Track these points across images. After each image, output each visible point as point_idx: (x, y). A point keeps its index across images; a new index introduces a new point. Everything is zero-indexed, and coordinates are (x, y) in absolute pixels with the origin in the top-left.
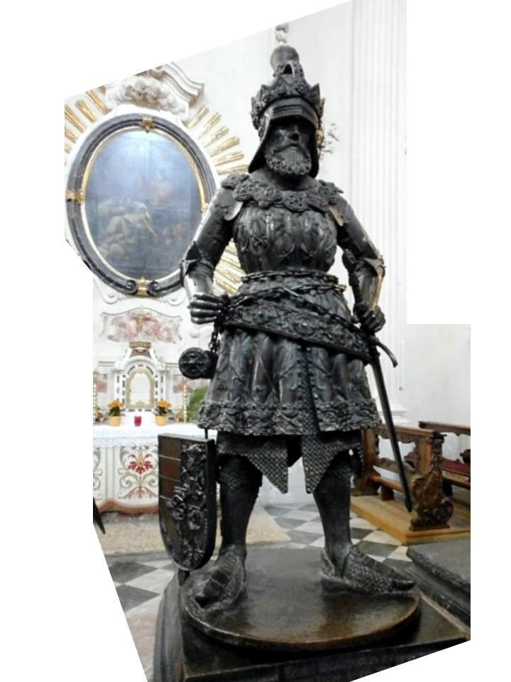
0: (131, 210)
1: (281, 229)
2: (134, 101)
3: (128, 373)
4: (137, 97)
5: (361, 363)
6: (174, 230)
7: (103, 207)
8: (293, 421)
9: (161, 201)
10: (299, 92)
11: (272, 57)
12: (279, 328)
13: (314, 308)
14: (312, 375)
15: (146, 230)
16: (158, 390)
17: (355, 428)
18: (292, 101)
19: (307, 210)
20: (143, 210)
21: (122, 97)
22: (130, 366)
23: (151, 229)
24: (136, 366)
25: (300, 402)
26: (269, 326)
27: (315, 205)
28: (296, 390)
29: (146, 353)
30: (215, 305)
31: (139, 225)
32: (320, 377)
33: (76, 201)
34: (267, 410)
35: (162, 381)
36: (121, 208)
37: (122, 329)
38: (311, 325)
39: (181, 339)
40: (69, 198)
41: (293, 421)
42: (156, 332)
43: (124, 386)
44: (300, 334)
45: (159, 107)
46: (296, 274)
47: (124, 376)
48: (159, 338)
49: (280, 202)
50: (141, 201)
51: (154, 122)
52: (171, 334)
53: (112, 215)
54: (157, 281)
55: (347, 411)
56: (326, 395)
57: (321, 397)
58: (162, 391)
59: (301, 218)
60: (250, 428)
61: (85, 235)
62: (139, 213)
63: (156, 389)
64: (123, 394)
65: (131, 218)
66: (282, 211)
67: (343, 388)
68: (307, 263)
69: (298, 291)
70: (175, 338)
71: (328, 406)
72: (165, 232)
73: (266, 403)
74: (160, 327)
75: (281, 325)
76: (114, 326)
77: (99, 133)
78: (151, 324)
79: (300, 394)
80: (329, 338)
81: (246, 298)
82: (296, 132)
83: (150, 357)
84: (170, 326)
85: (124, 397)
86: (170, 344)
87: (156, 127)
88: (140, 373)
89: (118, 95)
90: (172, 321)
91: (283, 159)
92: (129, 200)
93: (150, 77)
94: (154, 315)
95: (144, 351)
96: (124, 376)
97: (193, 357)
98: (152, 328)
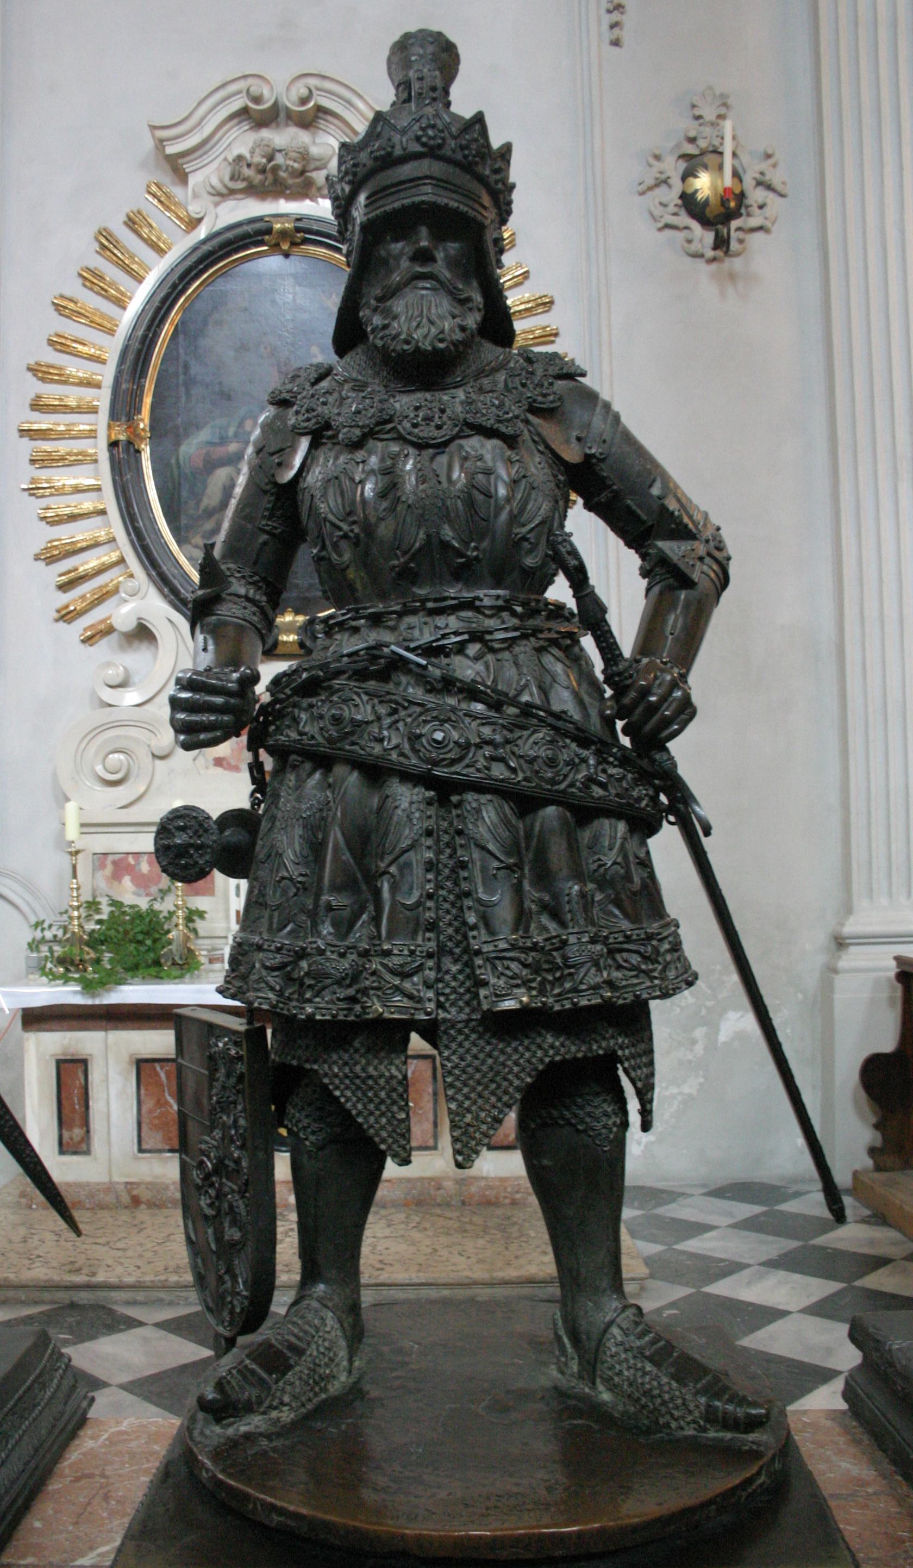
1: (391, 496)
2: (253, 191)
4: (258, 178)
5: (622, 827)
7: (192, 448)
8: (407, 985)
10: (424, 145)
11: (389, 62)
12: (377, 749)
13: (471, 692)
14: (463, 866)
17: (584, 1002)
18: (407, 170)
19: (457, 437)
21: (226, 186)
25: (428, 935)
26: (353, 744)
27: (480, 420)
28: (419, 904)
30: (219, 700)
32: (484, 869)
33: (129, 443)
34: (353, 957)
38: (455, 735)
40: (113, 438)
41: (407, 985)
44: (428, 761)
45: (314, 190)
46: (430, 605)
49: (389, 426)
51: (298, 230)
53: (211, 465)
55: (565, 958)
56: (504, 913)
57: (486, 920)
59: (443, 459)
60: (309, 1001)
61: (153, 521)
66: (395, 448)
67: (556, 896)
68: (464, 572)
69: (431, 651)
71: (503, 945)
73: (351, 940)
75: (381, 740)
77: (175, 277)
79: (430, 915)
80: (509, 767)
81: (305, 675)
82: (424, 243)
87: (305, 241)
89: (215, 182)
91: (395, 317)
93: (287, 125)
97: (183, 829)
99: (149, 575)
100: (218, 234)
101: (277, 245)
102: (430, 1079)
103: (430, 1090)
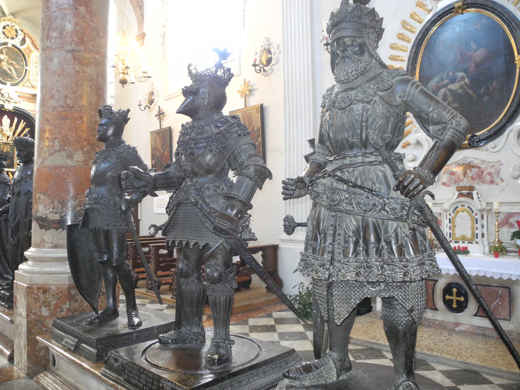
0: (453, 81)
3: (453, 212)
6: (491, 87)
9: (477, 65)
15: (467, 93)
16: (479, 225)
20: (463, 78)
22: (454, 207)
23: (470, 92)
24: (459, 206)
29: (470, 195)
31: (460, 91)
35: (482, 217)
36: (446, 81)
37: (452, 176)
39: (503, 181)
42: (480, 176)
43: (450, 222)
47: (450, 215)
48: (483, 182)
50: (460, 71)
52: (493, 177)
53: (439, 88)
54: (478, 134)
58: (483, 226)
62: (459, 82)
63: (476, 226)
64: (450, 229)
65: (453, 87)
70: (497, 180)
72: (482, 91)
74: (483, 173)
76: (446, 175)
77: (424, 29)
78: (475, 170)
83: (472, 198)
84: (492, 170)
85: (451, 231)
86: (494, 186)
87: (467, 8)
88: (463, 212)
90: (494, 166)
92: (451, 73)
94: (476, 162)
95: (468, 193)
96: (450, 215)
98: (476, 174)
99: (420, 126)
100: (437, 13)
101: (458, 11)
102: (508, 296)
103: (508, 299)
